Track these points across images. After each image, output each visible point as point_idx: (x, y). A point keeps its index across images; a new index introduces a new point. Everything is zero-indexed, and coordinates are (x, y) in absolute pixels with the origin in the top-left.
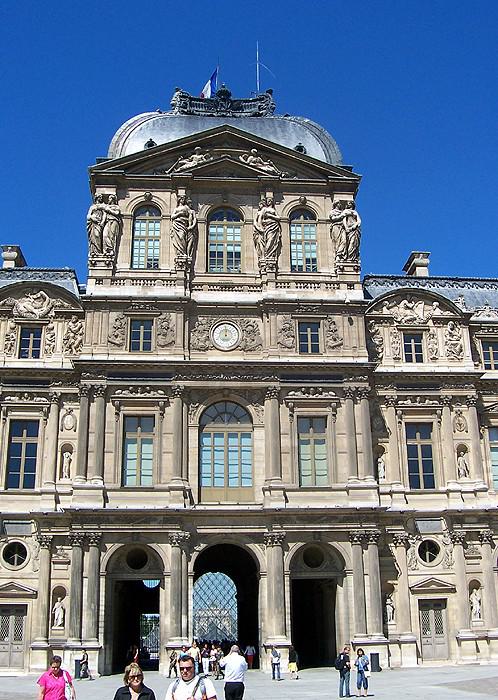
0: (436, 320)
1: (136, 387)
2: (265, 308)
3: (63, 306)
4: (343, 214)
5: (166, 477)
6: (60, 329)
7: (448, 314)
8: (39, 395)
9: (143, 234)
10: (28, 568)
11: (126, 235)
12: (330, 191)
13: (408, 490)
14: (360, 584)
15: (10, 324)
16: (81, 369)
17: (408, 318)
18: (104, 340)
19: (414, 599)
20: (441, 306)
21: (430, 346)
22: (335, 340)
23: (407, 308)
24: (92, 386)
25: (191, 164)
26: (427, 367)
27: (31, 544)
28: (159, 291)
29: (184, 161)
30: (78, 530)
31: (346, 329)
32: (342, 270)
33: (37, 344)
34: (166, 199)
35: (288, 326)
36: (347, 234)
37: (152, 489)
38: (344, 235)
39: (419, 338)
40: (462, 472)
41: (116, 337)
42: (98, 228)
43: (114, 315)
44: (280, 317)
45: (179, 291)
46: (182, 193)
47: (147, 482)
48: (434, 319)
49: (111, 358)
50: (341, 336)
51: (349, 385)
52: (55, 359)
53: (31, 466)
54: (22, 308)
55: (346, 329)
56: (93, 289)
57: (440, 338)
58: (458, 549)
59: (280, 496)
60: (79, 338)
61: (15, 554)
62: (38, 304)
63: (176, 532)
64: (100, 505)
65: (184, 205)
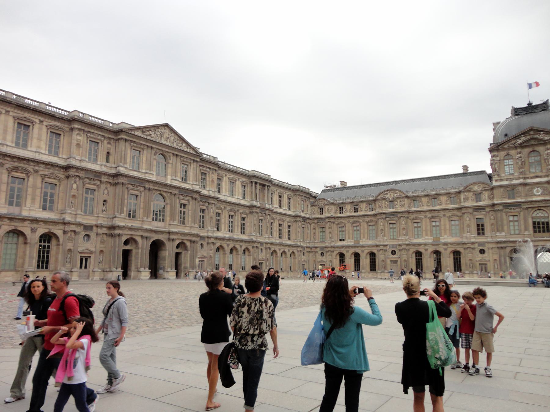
6: (486, 194)
10: (486, 255)
16: (494, 205)
27: (485, 249)
30: (500, 245)
33: (480, 198)
34: (512, 152)
37: (519, 234)
43: (502, 189)
45: (521, 181)
47: (517, 232)
53: (483, 229)
56: (495, 183)
61: (482, 251)
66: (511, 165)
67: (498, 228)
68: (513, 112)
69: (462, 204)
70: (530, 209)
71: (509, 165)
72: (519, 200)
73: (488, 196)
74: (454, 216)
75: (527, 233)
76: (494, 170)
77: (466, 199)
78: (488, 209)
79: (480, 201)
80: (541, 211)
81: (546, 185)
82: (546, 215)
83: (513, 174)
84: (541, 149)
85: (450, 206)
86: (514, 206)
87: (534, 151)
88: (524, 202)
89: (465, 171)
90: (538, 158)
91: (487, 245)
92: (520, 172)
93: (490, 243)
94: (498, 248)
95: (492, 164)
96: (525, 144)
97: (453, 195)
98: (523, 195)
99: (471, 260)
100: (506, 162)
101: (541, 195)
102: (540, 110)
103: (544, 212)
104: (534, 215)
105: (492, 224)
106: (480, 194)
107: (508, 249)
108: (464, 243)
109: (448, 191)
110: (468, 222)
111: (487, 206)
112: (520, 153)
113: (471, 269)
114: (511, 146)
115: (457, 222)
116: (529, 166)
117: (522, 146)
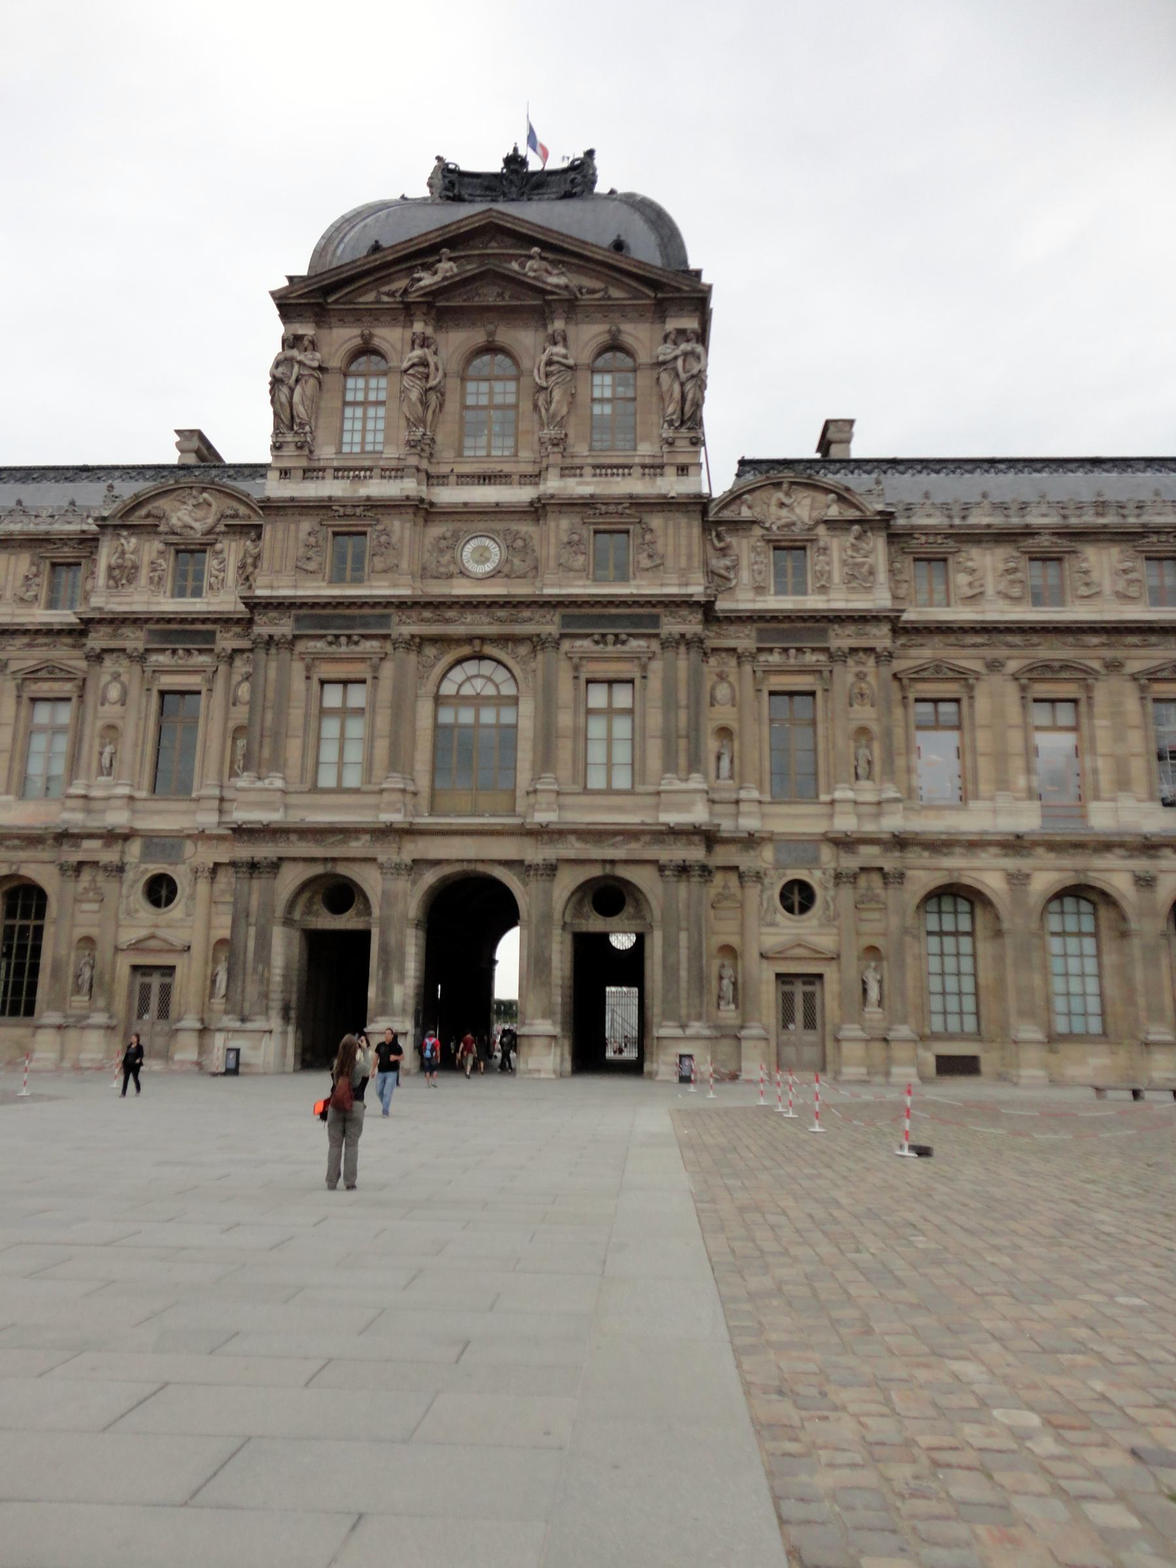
0: (831, 524)
1: (337, 637)
2: (538, 510)
4: (678, 352)
5: (379, 771)
6: (233, 550)
7: (852, 514)
8: (200, 651)
9: (360, 397)
10: (176, 910)
11: (330, 402)
12: (661, 310)
13: (767, 798)
14: (670, 944)
15: (157, 545)
17: (783, 521)
18: (290, 563)
19: (768, 973)
20: (841, 499)
21: (818, 568)
22: (650, 556)
23: (782, 505)
24: (271, 637)
25: (437, 278)
26: (814, 602)
27: (180, 874)
28: (377, 488)
31: (671, 541)
32: (671, 444)
33: (199, 576)
34: (390, 337)
35: (576, 537)
36: (682, 385)
40: (860, 771)
42: (285, 390)
43: (306, 525)
44: (565, 523)
45: (408, 487)
46: (418, 327)
47: (353, 779)
48: (826, 522)
49: (300, 593)
51: (671, 626)
52: (224, 600)
54: (174, 521)
55: (671, 541)
56: (275, 488)
57: (835, 555)
58: (847, 894)
59: (549, 804)
61: (160, 891)
62: (200, 514)
63: (386, 853)
64: (274, 817)
65: (422, 346)
66: (378, 403)
67: (252, 748)
68: (439, 182)
69: (96, 601)
70: (430, 651)
71: (365, 404)
72: (380, 589)
73: (243, 566)
74: (51, 671)
75: (395, 782)
76: (287, 422)
77: (122, 575)
78: (226, 641)
79: (197, 593)
80: (487, 667)
81: (525, 528)
82: (508, 689)
83: (382, 453)
84: (524, 340)
85: (40, 615)
86: (350, 622)
87: (491, 348)
88: (402, 605)
89: (191, 460)
90: (511, 386)
91: (189, 847)
92: (412, 444)
93: (201, 836)
94: (233, 864)
95: (276, 382)
96: (456, 302)
97: (67, 553)
98: (404, 565)
99: (88, 941)
100: (356, 388)
101: (495, 574)
102: (553, 196)
103: (501, 675)
104: (448, 688)
105: (239, 731)
106: (202, 548)
107: (291, 878)
108: (64, 837)
109: (41, 527)
110: (110, 712)
111: (226, 621)
112: (425, 342)
113: (81, 1000)
114: (385, 299)
115: (65, 714)
116: (462, 422)
117: (441, 308)
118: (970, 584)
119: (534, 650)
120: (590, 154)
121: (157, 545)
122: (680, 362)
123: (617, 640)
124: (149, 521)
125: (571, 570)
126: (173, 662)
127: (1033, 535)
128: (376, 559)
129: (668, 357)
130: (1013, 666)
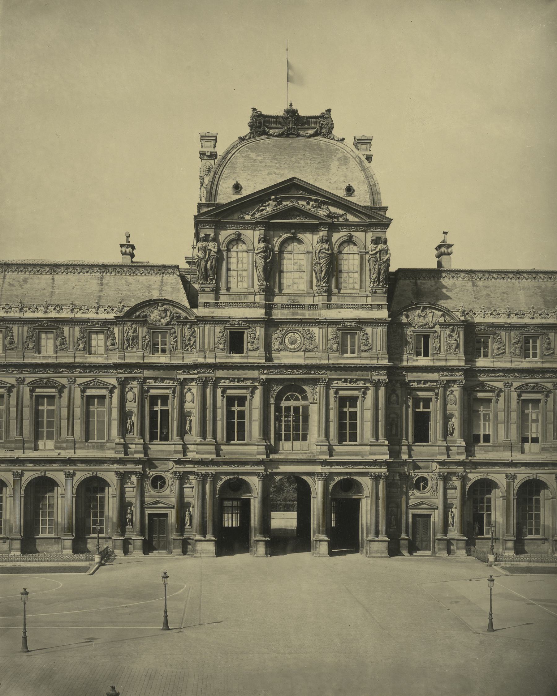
0: (441, 325)
3: (180, 317)
8: (168, 379)
21: (434, 345)
23: (419, 316)
27: (168, 476)
29: (263, 208)
36: (380, 265)
38: (377, 266)
39: (426, 338)
41: (221, 344)
50: (370, 342)
51: (374, 376)
57: (442, 339)
60: (193, 340)
65: (263, 242)
102: (311, 132)
118: (498, 349)
119: (315, 385)
120: (329, 111)
121: (145, 330)
122: (378, 254)
123: (351, 381)
124: (141, 318)
125: (333, 351)
126: (157, 384)
127: (526, 327)
128: (249, 344)
129: (374, 252)
130: (516, 385)
